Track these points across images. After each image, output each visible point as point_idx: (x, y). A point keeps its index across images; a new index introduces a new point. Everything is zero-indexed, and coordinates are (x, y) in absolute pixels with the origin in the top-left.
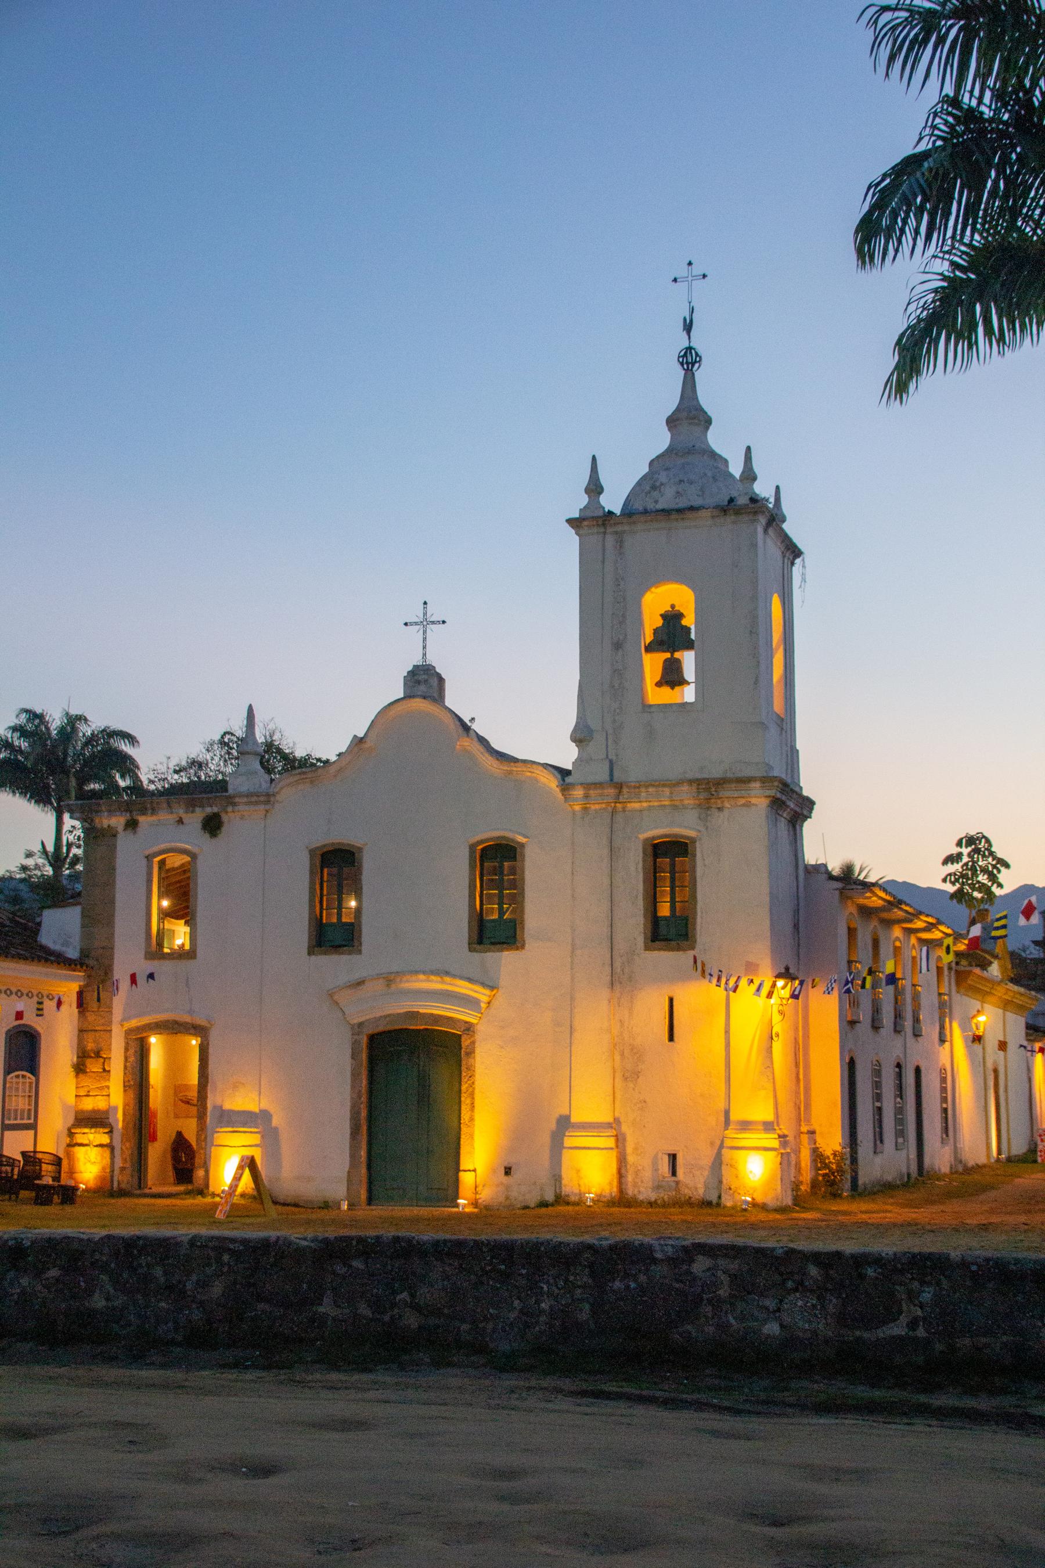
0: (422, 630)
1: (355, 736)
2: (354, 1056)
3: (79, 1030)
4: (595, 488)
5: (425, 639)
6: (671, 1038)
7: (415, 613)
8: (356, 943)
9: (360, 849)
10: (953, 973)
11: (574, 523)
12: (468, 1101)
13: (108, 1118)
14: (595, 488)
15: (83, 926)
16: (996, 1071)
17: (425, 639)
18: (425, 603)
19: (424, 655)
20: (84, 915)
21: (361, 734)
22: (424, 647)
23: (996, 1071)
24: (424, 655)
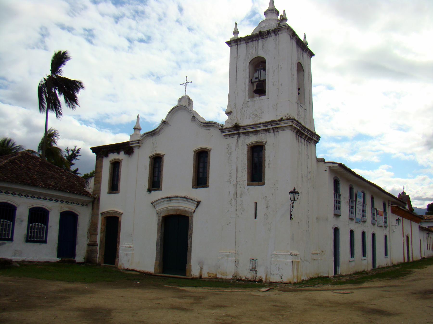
0: (185, 86)
1: (162, 120)
2: (158, 224)
3: (92, 215)
4: (236, 32)
5: (186, 88)
6: (256, 218)
7: (184, 81)
8: (160, 187)
9: (163, 156)
10: (390, 207)
11: (229, 43)
12: (190, 239)
13: (97, 242)
14: (236, 32)
15: (94, 184)
16: (408, 238)
17: (186, 88)
18: (187, 77)
19: (186, 93)
20: (95, 181)
21: (164, 119)
22: (186, 91)
23: (408, 238)
24: (186, 93)
